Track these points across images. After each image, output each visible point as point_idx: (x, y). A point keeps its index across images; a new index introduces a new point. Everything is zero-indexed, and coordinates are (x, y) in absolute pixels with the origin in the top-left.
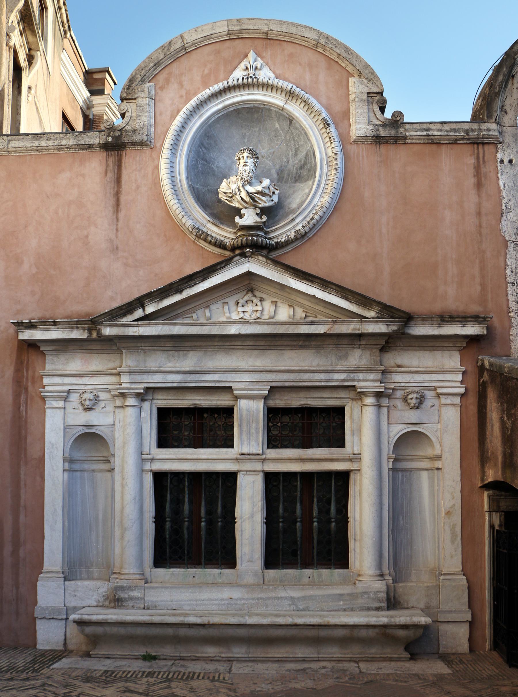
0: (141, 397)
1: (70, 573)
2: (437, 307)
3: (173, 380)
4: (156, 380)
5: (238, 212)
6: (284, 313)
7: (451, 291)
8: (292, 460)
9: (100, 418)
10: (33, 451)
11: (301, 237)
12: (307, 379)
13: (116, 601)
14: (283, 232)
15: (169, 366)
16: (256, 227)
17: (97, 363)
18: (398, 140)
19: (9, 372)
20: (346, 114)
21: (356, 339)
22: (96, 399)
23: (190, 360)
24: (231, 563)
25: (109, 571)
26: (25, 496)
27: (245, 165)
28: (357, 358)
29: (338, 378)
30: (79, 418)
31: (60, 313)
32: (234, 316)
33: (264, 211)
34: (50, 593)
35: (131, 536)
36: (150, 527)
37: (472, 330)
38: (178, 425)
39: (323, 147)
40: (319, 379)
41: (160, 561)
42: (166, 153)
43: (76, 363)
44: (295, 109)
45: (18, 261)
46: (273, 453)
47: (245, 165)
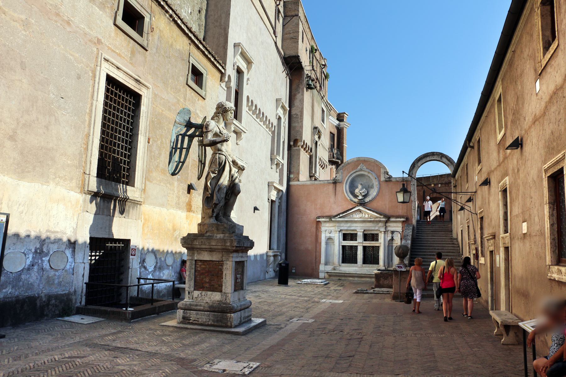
0: (340, 231)
1: (326, 264)
2: (398, 214)
3: (346, 228)
4: (342, 228)
5: (358, 196)
6: (367, 216)
7: (400, 211)
8: (368, 244)
9: (331, 235)
10: (319, 241)
11: (370, 201)
12: (371, 228)
13: (334, 269)
14: (367, 200)
15: (345, 225)
16: (362, 199)
17: (331, 224)
18: (390, 181)
19: (315, 226)
20: (380, 176)
21: (380, 221)
22: (331, 231)
23: (349, 225)
24: (356, 263)
25: (334, 264)
26: (318, 249)
27: (360, 187)
28: (380, 224)
29: (377, 228)
30: (328, 235)
31: (325, 215)
32: (357, 217)
33: (363, 196)
34: (322, 267)
35: (337, 257)
36: (341, 256)
37: (402, 219)
38: (346, 237)
39: (376, 183)
40: (373, 228)
41: (343, 262)
42: (344, 185)
43: (327, 225)
44: (369, 175)
45: (317, 205)
46: (364, 242)
47: (360, 187)
